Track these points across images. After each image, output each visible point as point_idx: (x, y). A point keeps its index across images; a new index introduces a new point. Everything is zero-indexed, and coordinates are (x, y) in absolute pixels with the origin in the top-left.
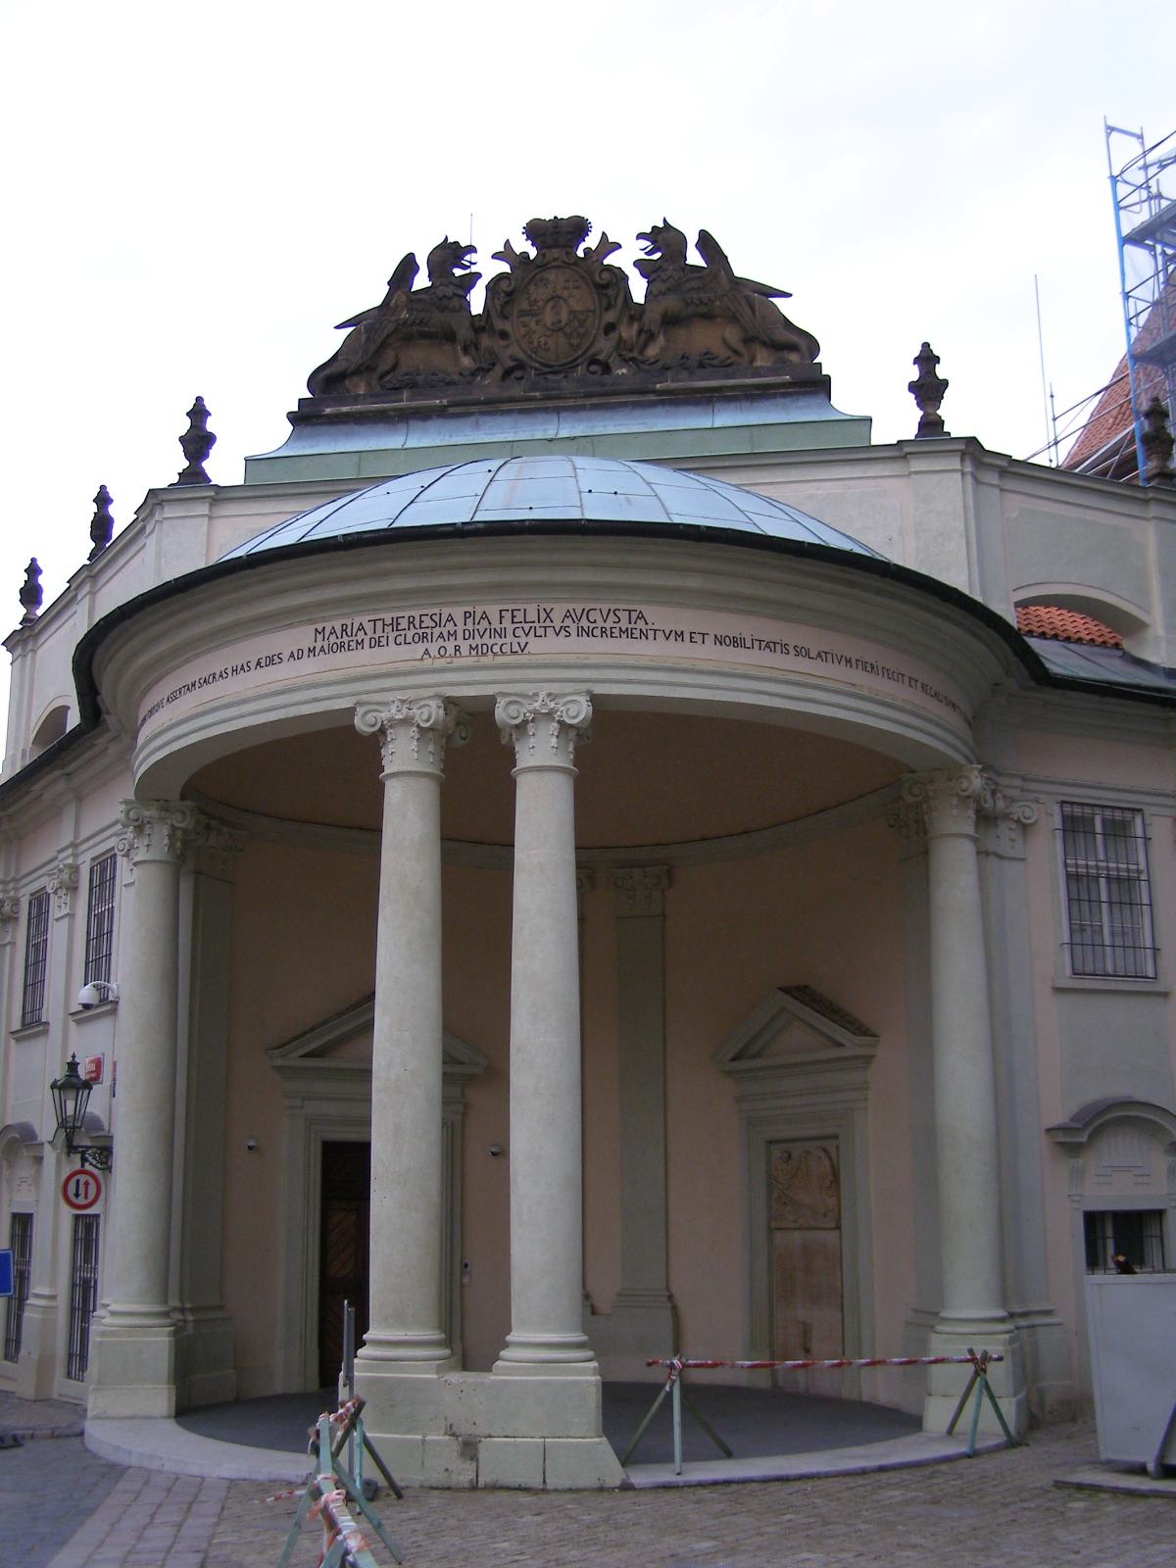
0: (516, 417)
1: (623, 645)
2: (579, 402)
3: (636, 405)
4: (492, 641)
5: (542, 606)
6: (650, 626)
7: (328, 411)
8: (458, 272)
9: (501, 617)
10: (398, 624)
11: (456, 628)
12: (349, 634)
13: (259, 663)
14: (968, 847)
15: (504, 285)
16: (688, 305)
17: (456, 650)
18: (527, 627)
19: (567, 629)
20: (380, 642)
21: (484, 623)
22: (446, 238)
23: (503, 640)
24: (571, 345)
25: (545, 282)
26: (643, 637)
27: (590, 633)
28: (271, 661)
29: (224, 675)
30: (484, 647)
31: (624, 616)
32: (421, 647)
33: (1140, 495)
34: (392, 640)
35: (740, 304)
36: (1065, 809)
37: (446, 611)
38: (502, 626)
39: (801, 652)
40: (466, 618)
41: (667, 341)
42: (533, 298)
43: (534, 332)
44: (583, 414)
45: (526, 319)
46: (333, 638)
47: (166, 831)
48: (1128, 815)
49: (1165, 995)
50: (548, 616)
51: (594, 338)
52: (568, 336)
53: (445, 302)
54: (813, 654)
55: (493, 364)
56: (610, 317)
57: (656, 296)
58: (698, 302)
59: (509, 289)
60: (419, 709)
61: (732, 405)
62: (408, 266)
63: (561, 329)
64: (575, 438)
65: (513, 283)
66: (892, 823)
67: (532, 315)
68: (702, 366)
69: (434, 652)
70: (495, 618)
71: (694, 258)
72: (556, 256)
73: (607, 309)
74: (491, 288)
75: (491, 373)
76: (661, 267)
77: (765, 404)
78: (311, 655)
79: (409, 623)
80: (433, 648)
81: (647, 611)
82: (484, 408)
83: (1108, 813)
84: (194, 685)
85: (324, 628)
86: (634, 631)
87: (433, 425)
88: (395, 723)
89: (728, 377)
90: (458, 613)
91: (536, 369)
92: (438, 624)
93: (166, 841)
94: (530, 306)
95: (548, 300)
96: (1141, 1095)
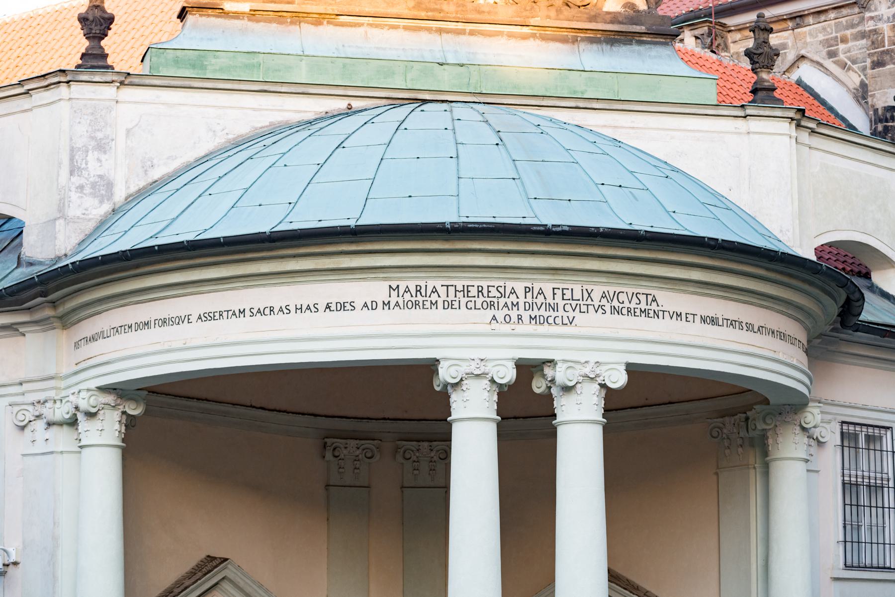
2: (460, 26)
4: (546, 314)
5: (585, 287)
6: (660, 308)
9: (554, 294)
10: (468, 291)
11: (518, 300)
12: (423, 294)
13: (328, 307)
14: (801, 466)
17: (519, 319)
18: (574, 303)
19: (603, 307)
20: (452, 305)
21: (541, 297)
23: (556, 314)
26: (656, 316)
28: (342, 307)
29: (286, 311)
30: (542, 318)
31: (643, 298)
32: (490, 313)
36: (844, 427)
37: (510, 285)
38: (555, 301)
39: (750, 327)
40: (526, 292)
46: (407, 296)
47: (116, 415)
48: (883, 431)
50: (589, 296)
54: (756, 330)
66: (715, 434)
69: (500, 315)
70: (549, 294)
77: (624, 49)
78: (386, 308)
79: (479, 292)
80: (500, 315)
81: (660, 296)
83: (870, 430)
85: (398, 286)
86: (650, 311)
90: (519, 287)
92: (503, 295)
93: (117, 426)
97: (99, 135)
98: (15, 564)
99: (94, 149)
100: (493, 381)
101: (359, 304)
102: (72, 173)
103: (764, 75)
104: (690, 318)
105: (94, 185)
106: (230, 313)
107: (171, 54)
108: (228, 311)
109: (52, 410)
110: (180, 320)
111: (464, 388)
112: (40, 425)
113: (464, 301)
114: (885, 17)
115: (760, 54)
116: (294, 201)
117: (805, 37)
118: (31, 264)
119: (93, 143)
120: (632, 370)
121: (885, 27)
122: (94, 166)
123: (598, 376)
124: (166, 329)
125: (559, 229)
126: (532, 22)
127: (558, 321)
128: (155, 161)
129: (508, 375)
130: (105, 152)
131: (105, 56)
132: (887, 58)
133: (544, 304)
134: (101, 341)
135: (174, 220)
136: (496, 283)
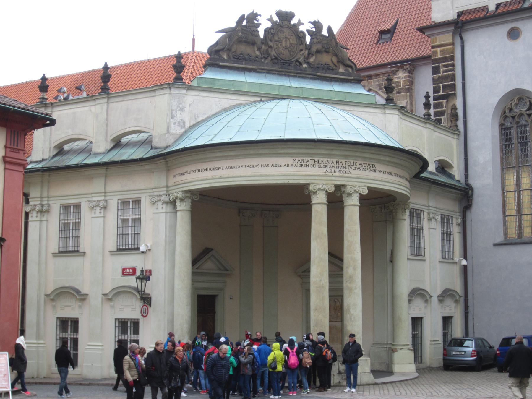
0: (278, 76)
1: (371, 173)
2: (295, 75)
3: (311, 78)
4: (343, 170)
6: (376, 169)
7: (221, 64)
8: (256, 22)
9: (345, 163)
10: (319, 162)
13: (272, 165)
15: (272, 31)
16: (323, 47)
18: (351, 166)
22: (253, 11)
23: (346, 170)
24: (290, 54)
25: (284, 32)
27: (364, 170)
28: (277, 165)
31: (371, 165)
32: (325, 169)
33: (425, 121)
34: (317, 166)
35: (338, 51)
37: (332, 160)
41: (316, 57)
42: (280, 36)
43: (279, 48)
44: (296, 79)
45: (277, 43)
46: (299, 163)
47: (190, 200)
49: (424, 260)
51: (297, 53)
52: (289, 51)
53: (254, 33)
55: (268, 56)
56: (301, 47)
57: (314, 44)
58: (326, 48)
59: (273, 32)
60: (327, 186)
61: (337, 83)
62: (242, 18)
63: (288, 49)
64: (296, 88)
65: (275, 31)
66: (372, 211)
67: (279, 42)
68: (328, 68)
69: (329, 170)
71: (325, 33)
72: (286, 24)
73: (300, 45)
74: (267, 31)
75: (267, 60)
76: (316, 34)
78: (292, 166)
80: (329, 170)
81: (377, 165)
82: (267, 71)
84: (242, 166)
85: (296, 159)
87: (253, 74)
88: (320, 189)
89: (336, 74)
90: (335, 161)
91: (281, 61)
93: (190, 204)
94: (278, 38)
95: (283, 38)
96: (422, 287)
97: (181, 106)
98: (150, 250)
99: (179, 110)
100: (327, 191)
101: (283, 164)
102: (172, 118)
103: (390, 95)
104: (384, 172)
105: (179, 123)
106: (238, 167)
107: (204, 80)
108: (237, 166)
109: (165, 198)
110: (219, 169)
111: (317, 193)
112: (160, 204)
113: (317, 165)
114: (401, 77)
115: (389, 88)
116: (260, 130)
117: (372, 83)
118: (156, 148)
119: (179, 108)
120: (370, 189)
121: (401, 81)
122: (179, 116)
123: (359, 191)
124: (213, 171)
125: (351, 142)
126: (319, 74)
127: (347, 172)
128: (199, 115)
129: (332, 189)
130: (183, 112)
131: (182, 79)
132: (402, 91)
133: (342, 167)
134: (186, 175)
135: (216, 135)
136: (328, 159)
